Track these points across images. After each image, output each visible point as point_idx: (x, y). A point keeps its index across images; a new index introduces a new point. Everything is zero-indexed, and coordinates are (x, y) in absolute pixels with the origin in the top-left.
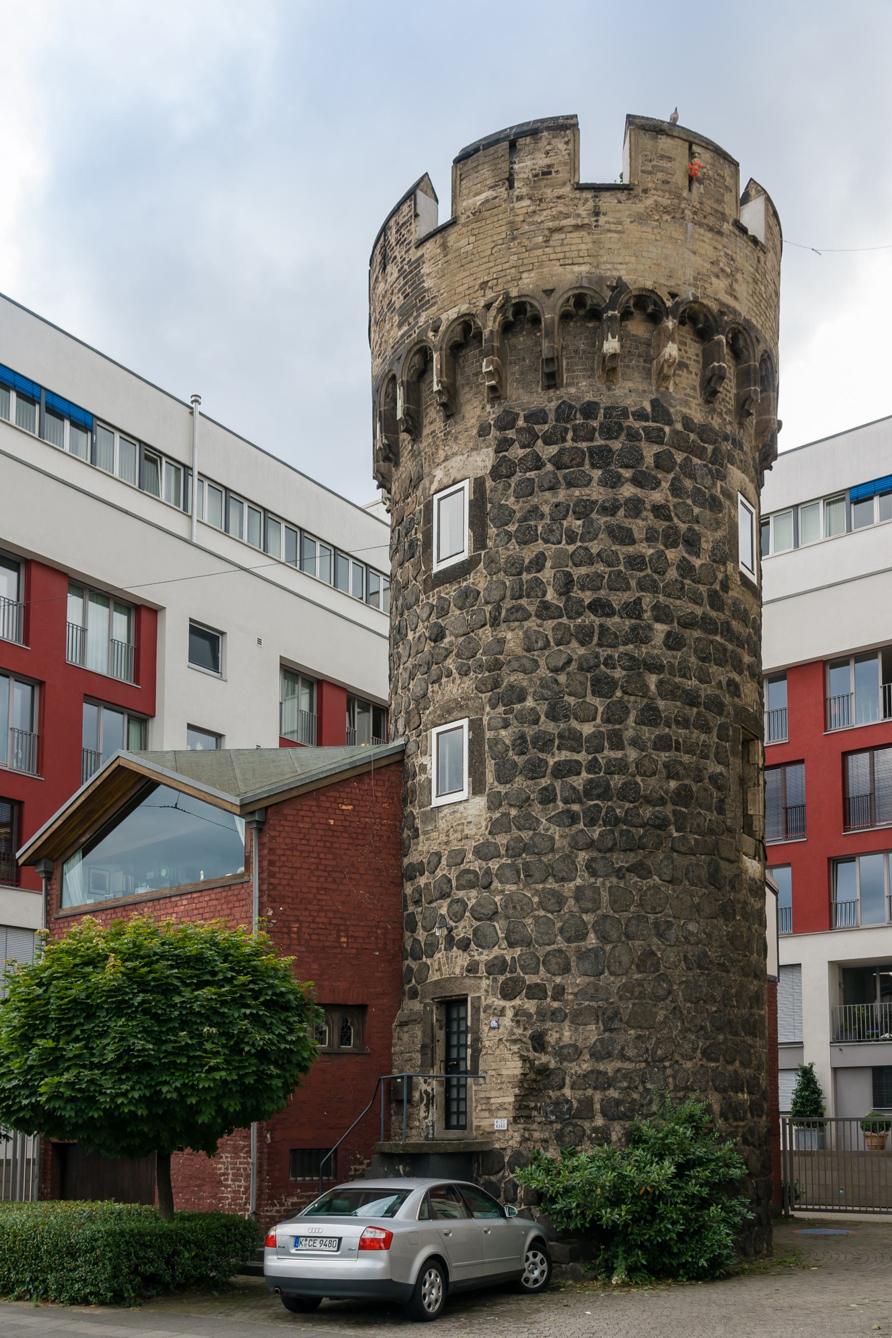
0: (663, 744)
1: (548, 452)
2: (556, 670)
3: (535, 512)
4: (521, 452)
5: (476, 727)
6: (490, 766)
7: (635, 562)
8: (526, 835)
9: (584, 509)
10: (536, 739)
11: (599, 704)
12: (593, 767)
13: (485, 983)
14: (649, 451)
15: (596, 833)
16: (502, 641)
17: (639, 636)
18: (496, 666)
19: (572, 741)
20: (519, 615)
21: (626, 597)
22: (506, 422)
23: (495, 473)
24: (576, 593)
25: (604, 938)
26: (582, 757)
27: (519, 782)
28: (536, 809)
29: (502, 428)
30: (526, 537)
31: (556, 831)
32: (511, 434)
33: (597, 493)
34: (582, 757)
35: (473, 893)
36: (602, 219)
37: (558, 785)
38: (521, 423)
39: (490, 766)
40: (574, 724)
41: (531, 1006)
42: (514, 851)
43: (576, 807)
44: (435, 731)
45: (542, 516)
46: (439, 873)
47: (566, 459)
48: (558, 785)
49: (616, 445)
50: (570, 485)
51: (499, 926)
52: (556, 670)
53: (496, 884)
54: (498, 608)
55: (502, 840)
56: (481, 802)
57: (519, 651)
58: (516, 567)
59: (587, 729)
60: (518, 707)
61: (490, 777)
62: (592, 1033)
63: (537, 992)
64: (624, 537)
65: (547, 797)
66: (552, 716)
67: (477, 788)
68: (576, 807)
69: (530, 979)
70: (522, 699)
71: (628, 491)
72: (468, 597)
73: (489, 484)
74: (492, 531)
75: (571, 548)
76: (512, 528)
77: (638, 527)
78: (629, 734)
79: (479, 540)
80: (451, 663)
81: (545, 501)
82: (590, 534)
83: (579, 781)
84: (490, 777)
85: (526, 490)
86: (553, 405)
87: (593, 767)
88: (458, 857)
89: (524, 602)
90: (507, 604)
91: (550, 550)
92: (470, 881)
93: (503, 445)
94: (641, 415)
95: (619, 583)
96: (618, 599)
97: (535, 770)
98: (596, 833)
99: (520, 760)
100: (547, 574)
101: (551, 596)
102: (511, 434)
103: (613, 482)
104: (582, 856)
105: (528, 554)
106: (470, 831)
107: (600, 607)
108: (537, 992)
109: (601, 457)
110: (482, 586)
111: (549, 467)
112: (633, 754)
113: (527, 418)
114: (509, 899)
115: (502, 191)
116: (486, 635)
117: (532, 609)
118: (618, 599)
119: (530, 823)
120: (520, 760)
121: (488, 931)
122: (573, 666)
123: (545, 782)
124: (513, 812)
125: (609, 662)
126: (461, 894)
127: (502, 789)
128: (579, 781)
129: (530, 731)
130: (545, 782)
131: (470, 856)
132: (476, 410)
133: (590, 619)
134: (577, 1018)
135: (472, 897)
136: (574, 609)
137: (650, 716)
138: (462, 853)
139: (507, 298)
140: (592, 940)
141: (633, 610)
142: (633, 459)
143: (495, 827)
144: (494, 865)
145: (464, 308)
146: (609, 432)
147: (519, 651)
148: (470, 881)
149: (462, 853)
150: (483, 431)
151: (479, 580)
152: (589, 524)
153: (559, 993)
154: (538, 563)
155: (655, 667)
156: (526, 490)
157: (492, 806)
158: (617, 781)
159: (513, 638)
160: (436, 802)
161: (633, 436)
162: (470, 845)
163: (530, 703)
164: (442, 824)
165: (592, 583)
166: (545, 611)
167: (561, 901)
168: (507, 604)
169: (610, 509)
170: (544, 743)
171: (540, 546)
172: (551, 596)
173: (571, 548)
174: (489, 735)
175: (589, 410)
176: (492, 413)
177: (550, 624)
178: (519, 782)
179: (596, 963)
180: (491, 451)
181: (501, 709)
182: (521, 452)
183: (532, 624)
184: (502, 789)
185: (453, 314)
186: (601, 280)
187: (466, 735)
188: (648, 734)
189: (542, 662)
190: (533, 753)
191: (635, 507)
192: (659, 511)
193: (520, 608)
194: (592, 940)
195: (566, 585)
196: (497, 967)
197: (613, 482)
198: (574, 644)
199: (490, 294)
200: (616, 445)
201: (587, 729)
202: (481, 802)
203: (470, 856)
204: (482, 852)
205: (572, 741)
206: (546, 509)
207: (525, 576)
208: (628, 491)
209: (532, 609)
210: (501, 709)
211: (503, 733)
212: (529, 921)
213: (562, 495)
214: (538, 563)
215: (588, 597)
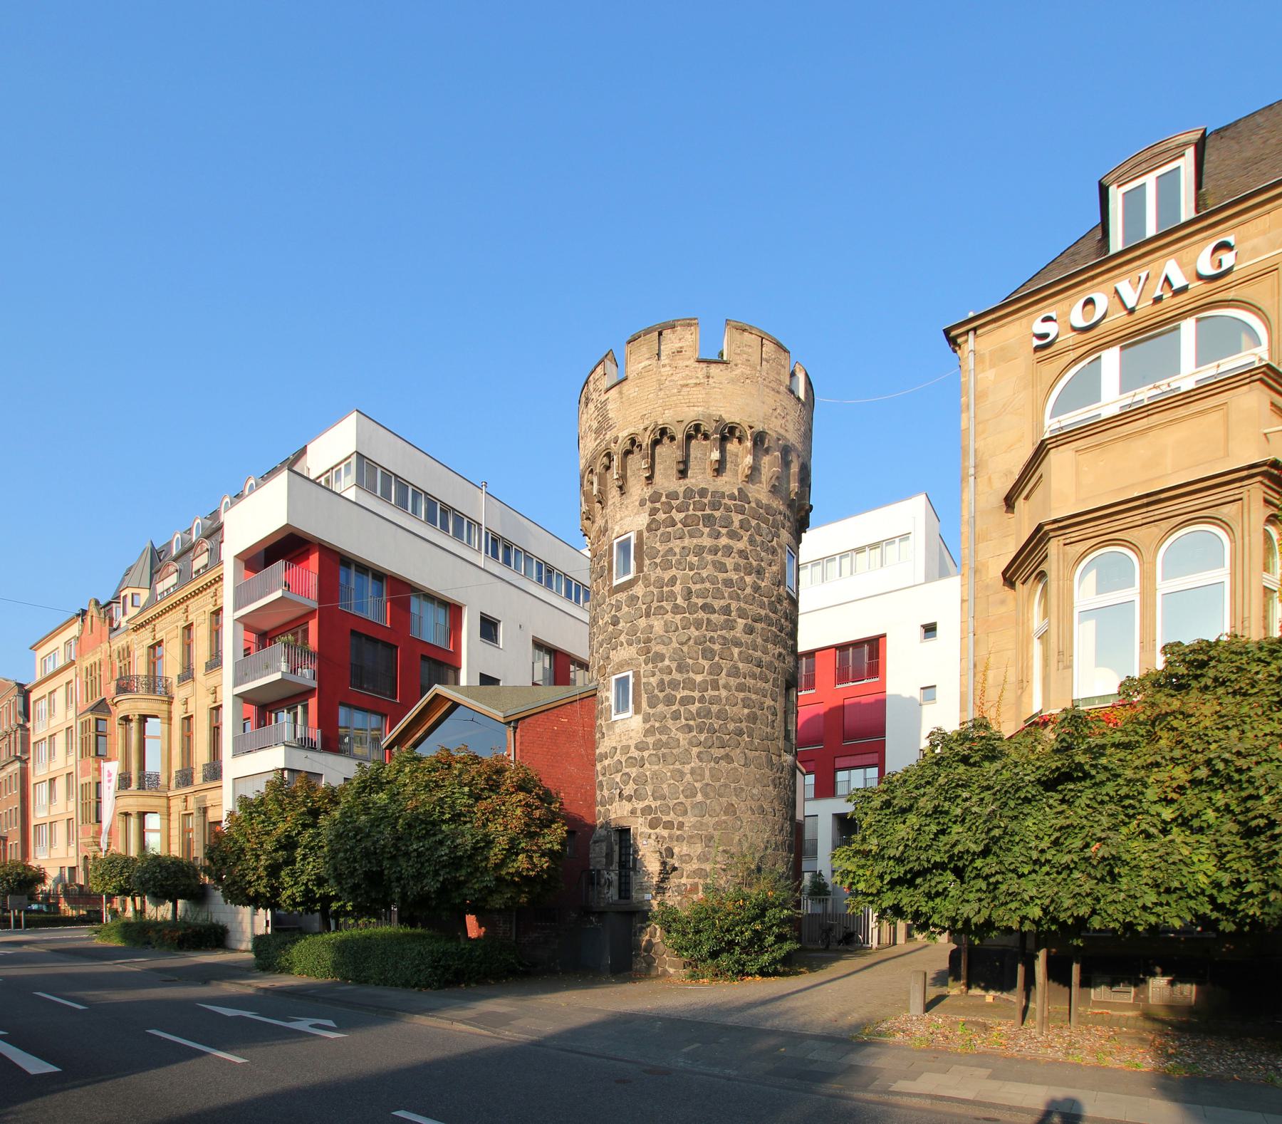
0: (741, 688)
1: (679, 516)
2: (682, 644)
4: (664, 516)
5: (636, 675)
6: (644, 697)
7: (728, 583)
8: (664, 738)
9: (699, 551)
10: (670, 683)
11: (706, 664)
12: (702, 700)
13: (640, 820)
15: (702, 737)
16: (651, 627)
17: (730, 626)
18: (648, 640)
19: (690, 685)
20: (661, 611)
21: (722, 603)
22: (655, 498)
23: (649, 529)
24: (694, 600)
25: (706, 795)
26: (696, 694)
27: (661, 708)
28: (670, 723)
29: (652, 502)
30: (667, 566)
31: (680, 736)
32: (658, 505)
33: (707, 542)
34: (696, 694)
35: (634, 770)
36: (711, 380)
37: (682, 709)
38: (664, 499)
39: (644, 697)
40: (691, 675)
41: (665, 833)
42: (658, 745)
43: (692, 723)
44: (614, 678)
45: (675, 554)
46: (616, 758)
47: (689, 521)
48: (682, 709)
49: (717, 514)
50: (691, 536)
51: (649, 789)
52: (682, 644)
53: (647, 765)
54: (650, 607)
55: (650, 740)
56: (639, 718)
57: (662, 633)
58: (660, 584)
59: (699, 678)
60: (660, 665)
61: (644, 705)
62: (698, 848)
63: (669, 825)
64: (722, 568)
65: (676, 716)
66: (680, 669)
67: (637, 711)
68: (692, 723)
69: (665, 818)
70: (663, 660)
71: (724, 541)
72: (633, 599)
73: (645, 534)
74: (647, 562)
75: (692, 573)
76: (658, 560)
77: (730, 563)
78: (721, 682)
79: (640, 568)
80: (623, 638)
81: (676, 545)
83: (694, 708)
84: (644, 705)
85: (666, 538)
86: (683, 489)
87: (702, 700)
88: (626, 749)
89: (664, 603)
90: (655, 604)
91: (679, 574)
92: (632, 761)
93: (653, 512)
94: (732, 497)
95: (718, 595)
96: (717, 604)
97: (669, 701)
98: (702, 737)
99: (661, 695)
100: (677, 588)
101: (680, 601)
102: (658, 505)
104: (695, 750)
105: (667, 576)
106: (632, 734)
107: (706, 608)
108: (669, 825)
109: (709, 520)
110: (640, 595)
111: (679, 525)
112: (724, 693)
113: (667, 497)
114: (655, 774)
115: (654, 361)
116: (642, 622)
117: (669, 608)
118: (717, 604)
119: (664, 730)
120: (661, 695)
121: (643, 792)
122: (692, 642)
123: (674, 708)
124: (657, 725)
125: (712, 640)
126: (627, 770)
127: (651, 711)
128: (694, 708)
129: (667, 678)
130: (674, 708)
131: (632, 749)
132: (637, 489)
134: (691, 840)
135: (634, 772)
136: (692, 609)
137: (735, 672)
138: (628, 747)
139: (656, 425)
140: (699, 797)
141: (726, 610)
142: (728, 523)
143: (648, 732)
144: (646, 754)
145: (632, 430)
146: (715, 506)
147: (662, 633)
148: (632, 761)
149: (628, 747)
150: (642, 503)
151: (639, 590)
153: (681, 826)
154: (673, 581)
155: (737, 643)
156: (666, 538)
157: (646, 720)
158: (715, 708)
159: (658, 624)
160: (614, 718)
161: (728, 509)
162: (632, 743)
163: (667, 662)
164: (617, 731)
166: (676, 609)
167: (682, 774)
168: (655, 604)
169: (714, 551)
170: (674, 685)
171: (673, 572)
172: (680, 601)
173: (692, 573)
174: (644, 680)
175: (703, 492)
176: (648, 492)
177: (679, 617)
178: (661, 708)
179: (702, 809)
180: (646, 515)
181: (650, 665)
182: (664, 516)
183: (669, 616)
184: (651, 711)
185: (625, 433)
186: (710, 416)
187: (631, 681)
188: (733, 682)
189: (674, 639)
190: (668, 691)
191: (728, 550)
192: (742, 553)
193: (662, 607)
194: (699, 797)
195: (688, 594)
196: (647, 810)
198: (693, 629)
199: (647, 422)
200: (717, 514)
201: (699, 678)
202: (639, 718)
203: (632, 749)
204: (641, 747)
205: (690, 685)
206: (677, 550)
207: (665, 589)
208: (724, 541)
209: (669, 608)
210: (650, 665)
211: (652, 679)
212: (665, 786)
213: (687, 542)
214: (673, 581)
215: (700, 602)
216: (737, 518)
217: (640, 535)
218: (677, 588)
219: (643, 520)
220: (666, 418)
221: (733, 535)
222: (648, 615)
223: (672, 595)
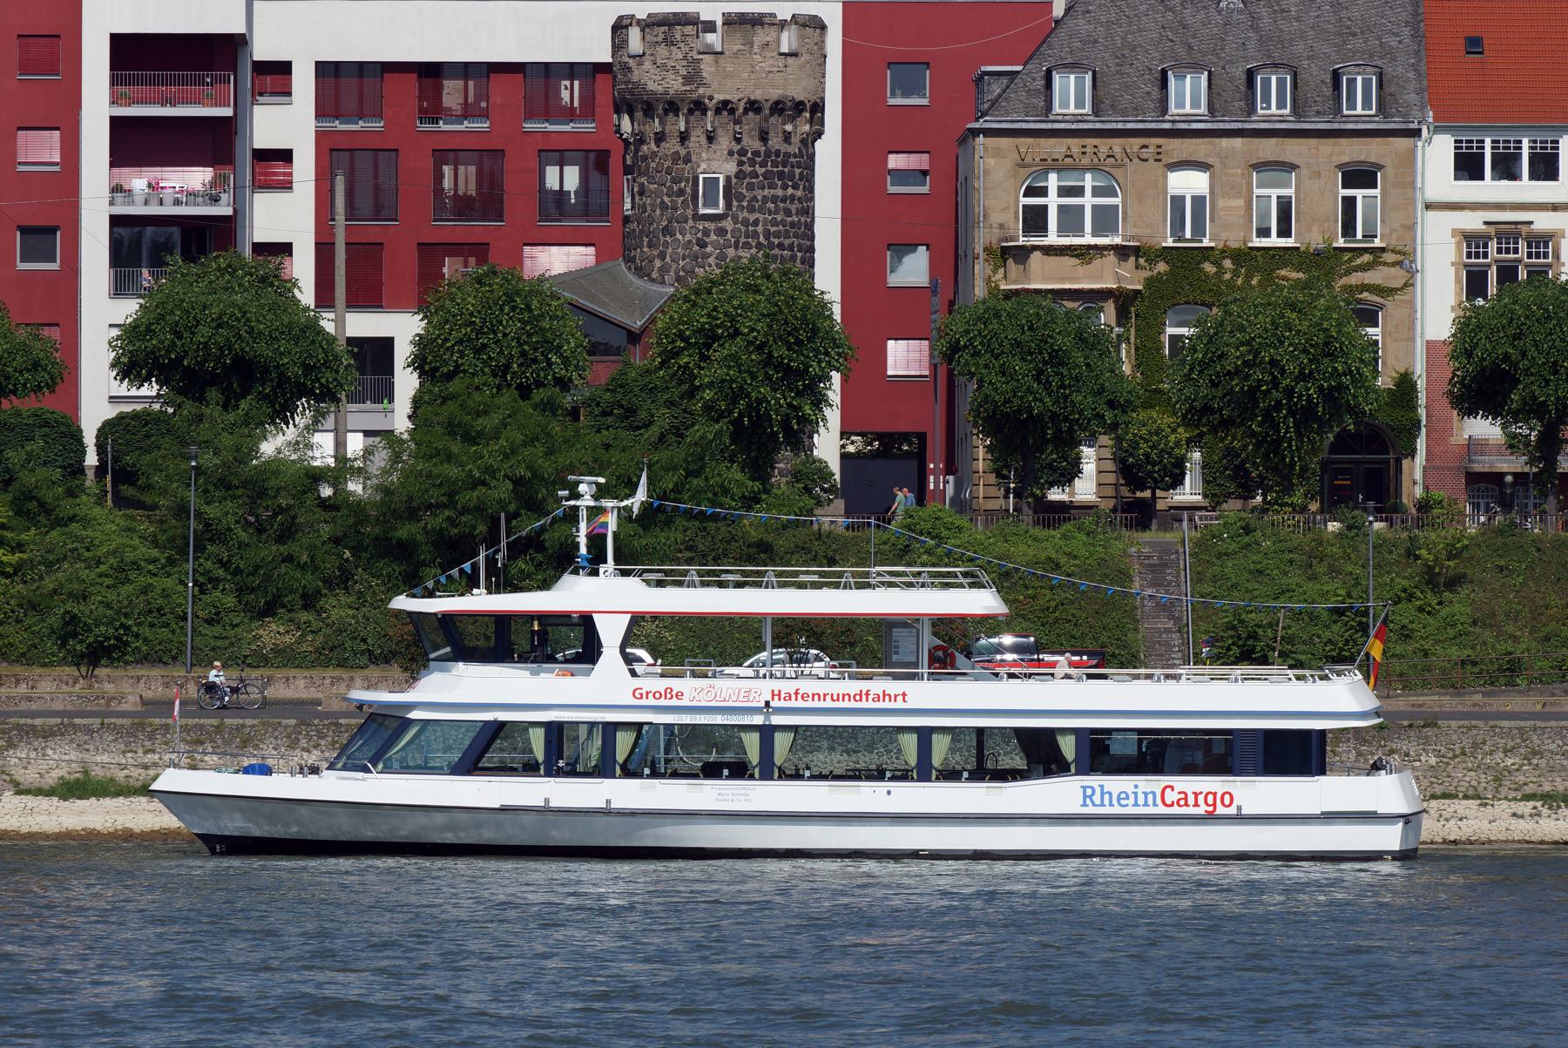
3: (755, 198)
7: (792, 225)
9: (774, 199)
14: (797, 171)
20: (747, 246)
22: (742, 152)
23: (737, 176)
30: (751, 209)
33: (780, 192)
58: (746, 222)
64: (788, 212)
71: (790, 191)
72: (722, 232)
73: (734, 180)
77: (793, 208)
79: (728, 206)
80: (711, 260)
81: (759, 194)
82: (777, 211)
85: (750, 187)
90: (743, 240)
91: (761, 217)
93: (740, 163)
96: (787, 242)
100: (760, 229)
101: (762, 239)
103: (785, 187)
105: (752, 218)
107: (781, 246)
109: (781, 175)
110: (729, 229)
116: (731, 252)
118: (787, 242)
133: (776, 251)
142: (791, 177)
145: (728, 97)
150: (731, 153)
151: (728, 224)
152: (777, 207)
154: (756, 223)
156: (750, 187)
165: (777, 235)
168: (743, 240)
175: (778, 153)
176: (736, 148)
183: (754, 251)
185: (722, 97)
191: (792, 198)
195: (767, 235)
197: (785, 187)
214: (756, 223)
215: (776, 241)
216: (797, 171)
217: (728, 179)
218: (760, 229)
219: (731, 167)
220: (757, 95)
221: (795, 187)
222: (736, 248)
223: (755, 235)
